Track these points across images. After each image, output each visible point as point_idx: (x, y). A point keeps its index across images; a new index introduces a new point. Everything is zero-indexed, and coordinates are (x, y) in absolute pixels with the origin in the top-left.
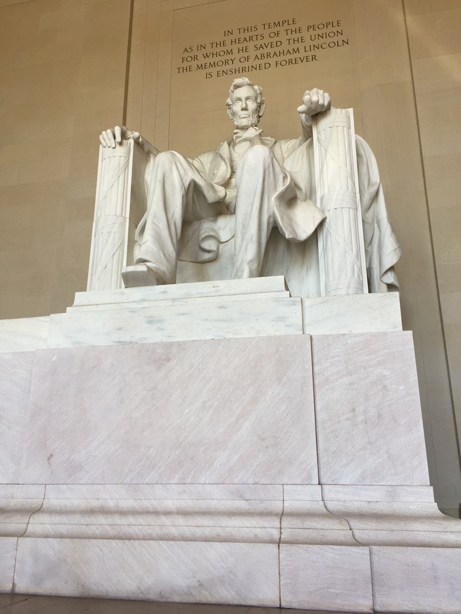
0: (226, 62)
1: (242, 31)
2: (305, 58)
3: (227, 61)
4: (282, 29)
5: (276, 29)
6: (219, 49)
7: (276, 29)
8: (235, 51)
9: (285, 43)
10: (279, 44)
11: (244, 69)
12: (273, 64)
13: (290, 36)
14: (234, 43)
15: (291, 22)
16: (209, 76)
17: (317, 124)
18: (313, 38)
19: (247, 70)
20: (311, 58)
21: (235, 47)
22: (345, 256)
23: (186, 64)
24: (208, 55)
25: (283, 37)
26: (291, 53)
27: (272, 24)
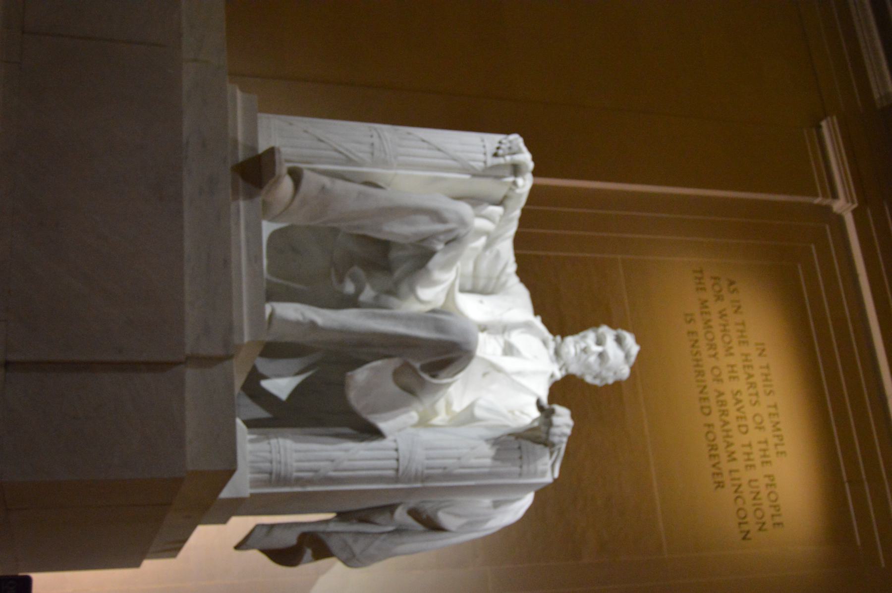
0: (712, 346)
1: (765, 371)
4: (768, 434)
5: (768, 424)
7: (768, 424)
8: (731, 360)
9: (745, 439)
10: (744, 429)
11: (701, 373)
13: (756, 448)
14: (744, 357)
15: (780, 449)
18: (753, 484)
19: (700, 378)
20: (719, 479)
21: (737, 360)
22: (327, 460)
23: (708, 283)
24: (724, 318)
25: (754, 436)
27: (776, 419)
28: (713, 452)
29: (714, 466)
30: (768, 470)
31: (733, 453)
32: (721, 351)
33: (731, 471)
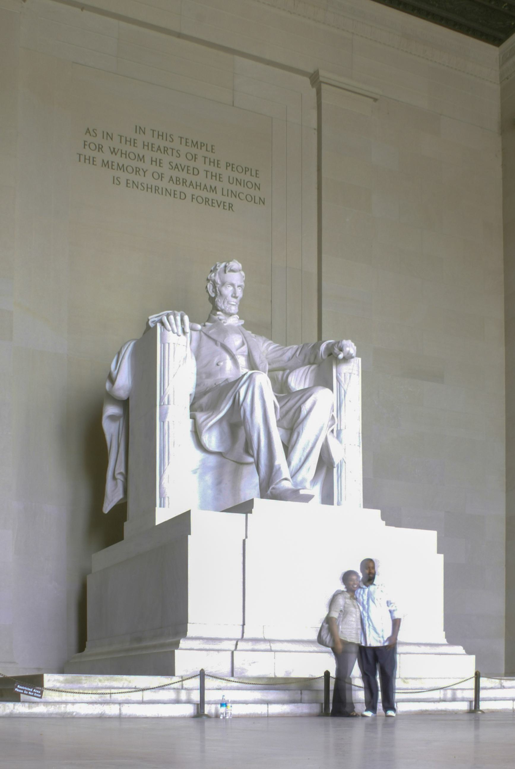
0: (137, 171)
2: (222, 203)
3: (138, 169)
6: (127, 148)
8: (148, 159)
9: (202, 174)
10: (196, 172)
11: (157, 189)
12: (189, 197)
14: (146, 147)
16: (116, 181)
17: (337, 365)
18: (231, 181)
19: (160, 191)
20: (227, 205)
21: (148, 154)
23: (88, 152)
24: (116, 150)
26: (209, 189)
28: (210, 202)
29: (219, 206)
30: (223, 164)
31: (211, 187)
32: (140, 165)
33: (223, 194)
